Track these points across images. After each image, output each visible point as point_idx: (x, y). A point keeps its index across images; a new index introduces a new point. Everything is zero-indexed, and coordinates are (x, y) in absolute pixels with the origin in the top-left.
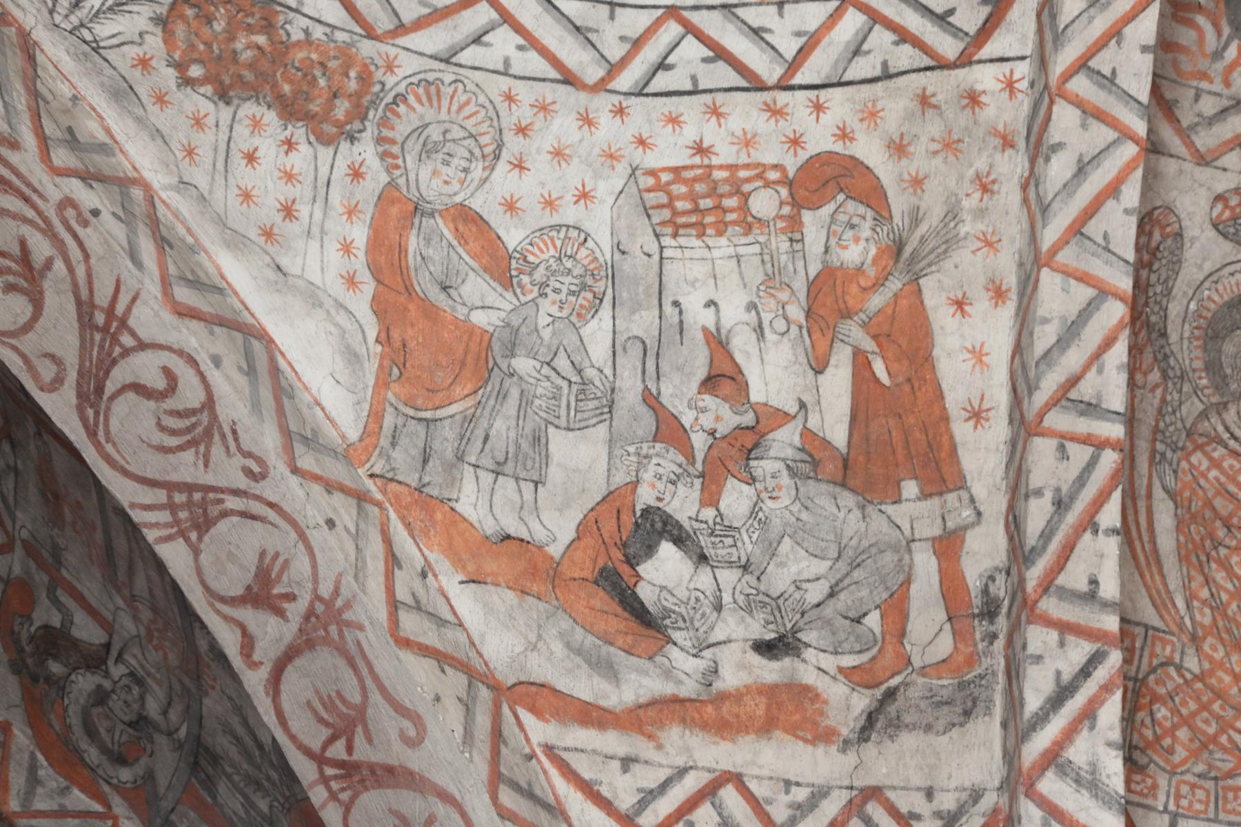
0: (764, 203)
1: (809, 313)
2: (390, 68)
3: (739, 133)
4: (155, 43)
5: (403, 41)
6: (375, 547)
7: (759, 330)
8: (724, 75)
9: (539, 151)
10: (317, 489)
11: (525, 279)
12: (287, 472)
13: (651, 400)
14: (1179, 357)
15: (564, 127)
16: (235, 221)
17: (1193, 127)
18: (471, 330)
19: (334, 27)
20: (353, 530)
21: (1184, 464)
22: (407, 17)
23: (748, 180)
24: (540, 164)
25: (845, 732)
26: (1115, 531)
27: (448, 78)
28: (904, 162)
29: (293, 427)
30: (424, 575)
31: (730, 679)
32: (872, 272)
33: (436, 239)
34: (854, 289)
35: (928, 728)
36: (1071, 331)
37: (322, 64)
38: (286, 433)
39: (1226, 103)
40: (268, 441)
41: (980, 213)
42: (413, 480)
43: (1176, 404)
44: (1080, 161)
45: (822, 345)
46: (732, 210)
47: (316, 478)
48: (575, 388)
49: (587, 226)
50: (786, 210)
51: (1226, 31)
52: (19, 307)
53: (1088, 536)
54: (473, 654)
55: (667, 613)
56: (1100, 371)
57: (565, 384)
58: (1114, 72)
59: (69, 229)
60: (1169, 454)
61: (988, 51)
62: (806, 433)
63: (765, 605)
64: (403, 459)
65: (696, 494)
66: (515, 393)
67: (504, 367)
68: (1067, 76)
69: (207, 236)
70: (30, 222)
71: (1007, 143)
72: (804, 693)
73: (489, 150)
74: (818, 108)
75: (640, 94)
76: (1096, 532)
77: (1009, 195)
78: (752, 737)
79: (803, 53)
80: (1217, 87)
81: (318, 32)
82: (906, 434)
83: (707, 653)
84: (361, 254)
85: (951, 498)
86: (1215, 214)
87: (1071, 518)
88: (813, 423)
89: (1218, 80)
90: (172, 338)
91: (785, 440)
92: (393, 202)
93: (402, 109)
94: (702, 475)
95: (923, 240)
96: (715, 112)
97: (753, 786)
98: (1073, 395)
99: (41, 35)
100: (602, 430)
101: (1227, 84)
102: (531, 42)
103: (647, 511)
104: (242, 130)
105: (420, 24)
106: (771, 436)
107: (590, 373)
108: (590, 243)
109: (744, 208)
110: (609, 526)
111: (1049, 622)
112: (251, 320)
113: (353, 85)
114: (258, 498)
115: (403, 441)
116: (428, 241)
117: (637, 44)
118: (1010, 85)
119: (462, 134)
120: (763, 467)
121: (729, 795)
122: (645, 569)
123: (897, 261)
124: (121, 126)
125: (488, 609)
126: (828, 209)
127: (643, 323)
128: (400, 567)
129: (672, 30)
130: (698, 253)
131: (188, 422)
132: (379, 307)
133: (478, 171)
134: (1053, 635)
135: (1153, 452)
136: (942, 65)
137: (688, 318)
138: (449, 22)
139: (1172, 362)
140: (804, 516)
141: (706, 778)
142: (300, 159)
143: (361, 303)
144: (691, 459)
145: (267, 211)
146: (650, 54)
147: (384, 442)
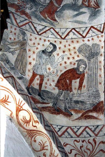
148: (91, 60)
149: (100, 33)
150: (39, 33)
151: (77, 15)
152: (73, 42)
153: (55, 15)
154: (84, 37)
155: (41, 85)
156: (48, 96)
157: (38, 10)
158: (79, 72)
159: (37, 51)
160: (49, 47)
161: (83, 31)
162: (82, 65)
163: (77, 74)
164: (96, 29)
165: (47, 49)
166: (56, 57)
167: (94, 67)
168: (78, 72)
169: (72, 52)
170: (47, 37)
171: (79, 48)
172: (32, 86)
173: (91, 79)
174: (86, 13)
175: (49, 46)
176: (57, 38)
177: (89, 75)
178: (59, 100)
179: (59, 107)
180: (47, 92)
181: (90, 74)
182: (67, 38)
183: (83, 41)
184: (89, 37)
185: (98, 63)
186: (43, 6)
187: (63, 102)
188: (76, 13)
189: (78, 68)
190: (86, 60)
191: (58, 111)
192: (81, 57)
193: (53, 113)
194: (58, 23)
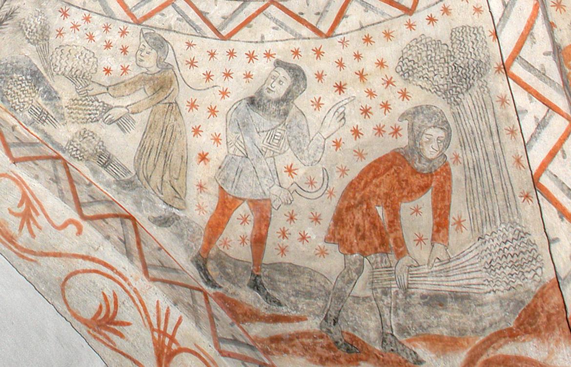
150: (224, 32)
152: (367, 40)
155: (259, 241)
156: (297, 288)
159: (223, 105)
160: (274, 78)
165: (265, 91)
166: (313, 117)
169: (376, 82)
170: (259, 39)
171: (402, 59)
172: (221, 248)
175: (274, 73)
176: (298, 37)
178: (349, 300)
179: (354, 330)
180: (292, 271)
182: (345, 30)
185: (497, 106)
187: (371, 308)
190: (441, 104)
191: (348, 350)
193: (327, 359)
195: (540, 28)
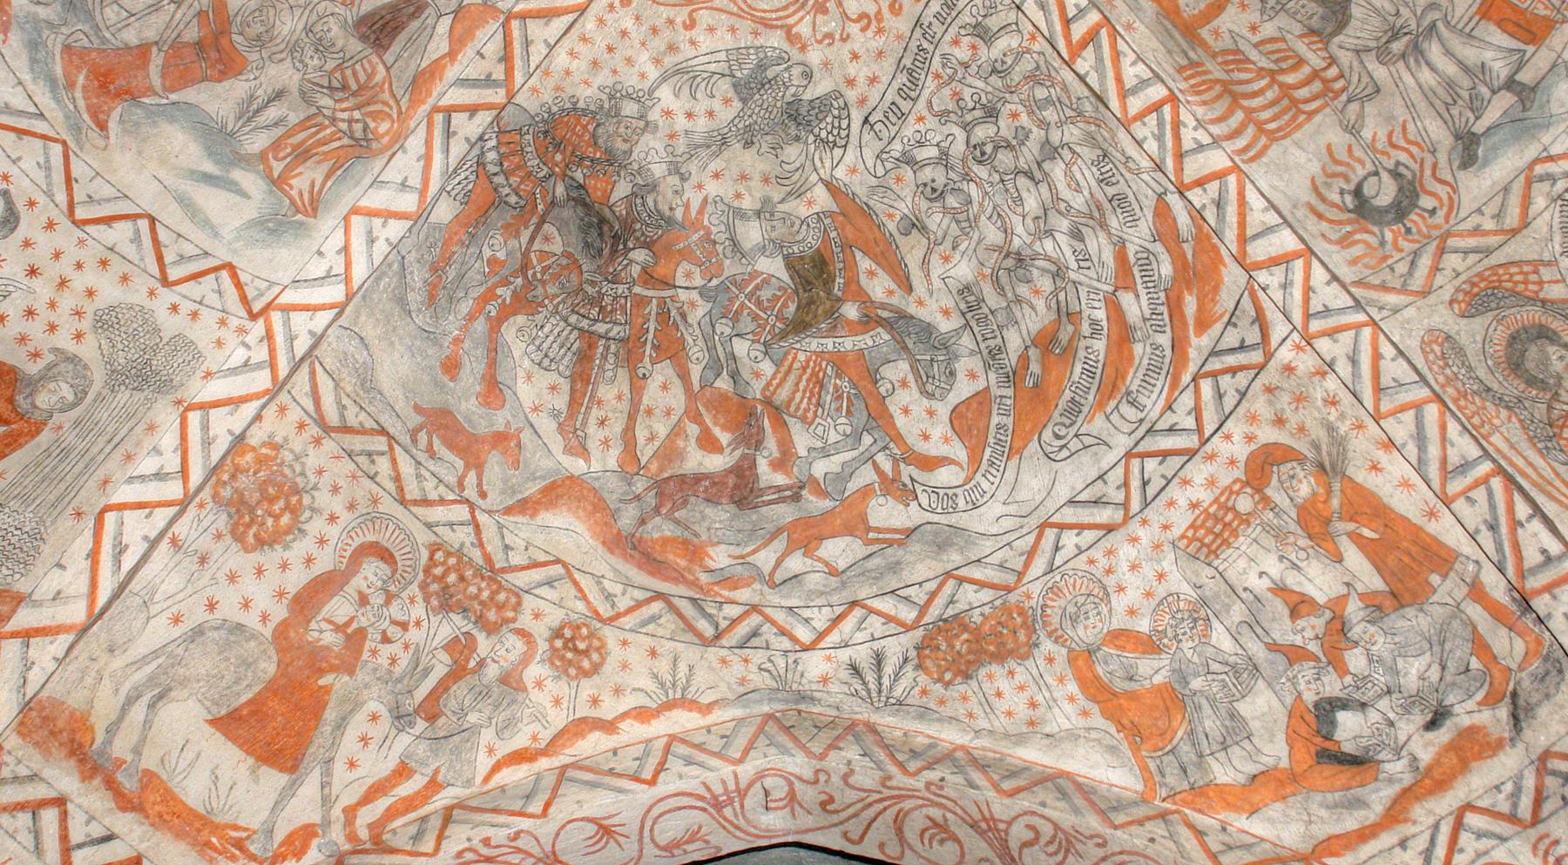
0: (1244, 504)
1: (1310, 537)
2: (1029, 597)
3: (1204, 482)
4: (923, 679)
5: (1025, 580)
6: (1185, 834)
7: (1295, 566)
8: (1176, 461)
9: (1124, 574)
10: (1134, 829)
11: (1165, 641)
12: (1113, 831)
13: (1273, 647)
14: (1507, 392)
15: (1127, 552)
16: (1012, 729)
17: (1405, 284)
18: (1159, 689)
19: (991, 602)
20: (1167, 834)
21: (1562, 442)
22: (1019, 567)
23: (1228, 499)
24: (1130, 579)
25: (1506, 735)
26: (1531, 517)
27: (1058, 578)
28: (1288, 425)
29: (1103, 807)
30: (1224, 829)
31: (1425, 757)
32: (1321, 491)
33: (1109, 659)
34: (1320, 506)
35: (1547, 696)
36: (1420, 438)
37: (999, 623)
38: (1102, 813)
39: (1410, 259)
40: (1093, 822)
41: (1342, 416)
42: (1186, 786)
43: (1529, 416)
44: (1349, 358)
45: (1330, 546)
46: (1233, 520)
47: (1131, 823)
48: (1231, 674)
49: (1173, 589)
50: (1257, 497)
51: (1376, 229)
52: (950, 846)
53: (1520, 531)
54: (1279, 850)
55: (1367, 749)
56: (1452, 445)
57: (1224, 676)
58: (1325, 306)
59: (939, 796)
60: (1549, 445)
61: (1274, 342)
62: (1362, 596)
63: (1414, 702)
64: (1173, 779)
65: (1334, 676)
66: (1203, 701)
67: (1188, 692)
68: (1306, 325)
69: (1005, 747)
70: (921, 806)
71: (1323, 374)
72: (1470, 733)
73: (1101, 595)
74: (1228, 437)
75: (1147, 505)
76: (1522, 526)
77: (1346, 398)
78: (1460, 777)
79: (1199, 419)
80: (1397, 256)
81: (987, 610)
82: (1410, 554)
83: (1404, 753)
84: (1080, 696)
85: (1457, 566)
86: (1457, 311)
87: (1504, 530)
88: (1360, 588)
89: (1394, 253)
90: (1017, 810)
91: (1354, 609)
92: (1076, 659)
93: (1049, 611)
94: (1330, 663)
95: (1329, 454)
96: (1186, 482)
97: (1480, 803)
98: (1450, 468)
99: (875, 718)
100: (1261, 684)
101: (1401, 251)
102: (1081, 527)
103: (1317, 705)
104: (986, 686)
105: (1027, 565)
106: (1346, 613)
107: (1232, 659)
108: (1182, 597)
109: (1237, 514)
110: (1304, 731)
111: (1539, 592)
112: (1052, 771)
113: (1019, 620)
114: (1113, 854)
115: (1168, 770)
116: (1106, 663)
117: (1126, 484)
118: (1298, 348)
119: (1084, 598)
120: (1356, 632)
121: (1472, 819)
122: (1339, 735)
123: (1327, 474)
124: (932, 730)
125: (1271, 821)
126: (1275, 478)
127: (1238, 612)
128: (1206, 835)
129: (1135, 463)
130: (1235, 555)
131: (1056, 844)
132: (1106, 715)
133: (1105, 610)
134: (1547, 597)
135: (1540, 451)
136: (1261, 368)
137: (1257, 591)
138: (1039, 552)
139: (1507, 399)
140: (1397, 639)
141: (1451, 820)
142: (1021, 677)
143: (1099, 721)
144: (1317, 659)
145: (1023, 711)
146: (1135, 484)
147: (1157, 778)
148: (120, 395)
149: (245, 314)
151: (208, 179)
152: (104, 263)
153: (119, 109)
154: (165, 282)
157: (64, 30)
158: (29, 401)
161: (182, 257)
162: (64, 386)
163: (11, 400)
164: (239, 285)
167: (110, 429)
168: (20, 398)
169: (67, 302)
171: (112, 308)
173: (55, 468)
174: (248, 197)
176: (49, 194)
177: (63, 446)
181: (66, 443)
183: (152, 293)
184: (184, 296)
186: (98, 37)
188: (209, 167)
189: (34, 385)
192: (88, 350)
194: (105, 149)
195: (249, 409)
